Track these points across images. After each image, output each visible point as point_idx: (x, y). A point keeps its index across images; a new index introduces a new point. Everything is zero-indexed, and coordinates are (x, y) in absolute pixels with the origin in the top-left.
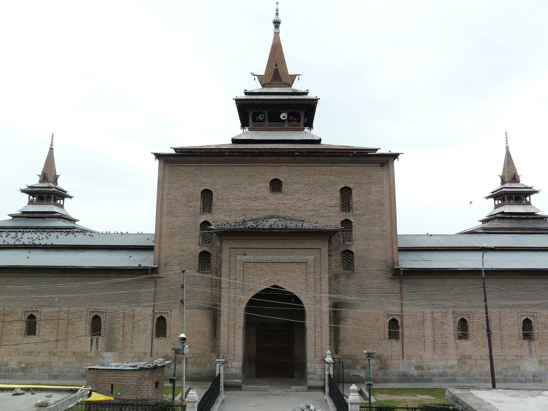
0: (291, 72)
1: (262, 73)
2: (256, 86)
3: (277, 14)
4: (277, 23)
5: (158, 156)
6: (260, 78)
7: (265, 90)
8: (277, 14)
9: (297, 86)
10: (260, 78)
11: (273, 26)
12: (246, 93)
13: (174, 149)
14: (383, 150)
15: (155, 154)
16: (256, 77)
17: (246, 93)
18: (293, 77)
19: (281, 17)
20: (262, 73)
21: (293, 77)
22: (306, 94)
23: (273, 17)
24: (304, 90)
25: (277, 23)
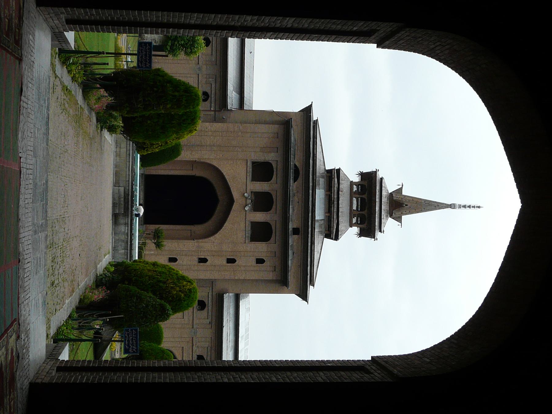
0: (404, 217)
1: (404, 193)
2: (390, 186)
5: (308, 111)
6: (400, 191)
7: (384, 193)
9: (389, 224)
10: (400, 191)
12: (382, 179)
13: (317, 120)
15: (310, 106)
16: (401, 186)
17: (382, 179)
18: (399, 219)
20: (404, 193)
21: (399, 219)
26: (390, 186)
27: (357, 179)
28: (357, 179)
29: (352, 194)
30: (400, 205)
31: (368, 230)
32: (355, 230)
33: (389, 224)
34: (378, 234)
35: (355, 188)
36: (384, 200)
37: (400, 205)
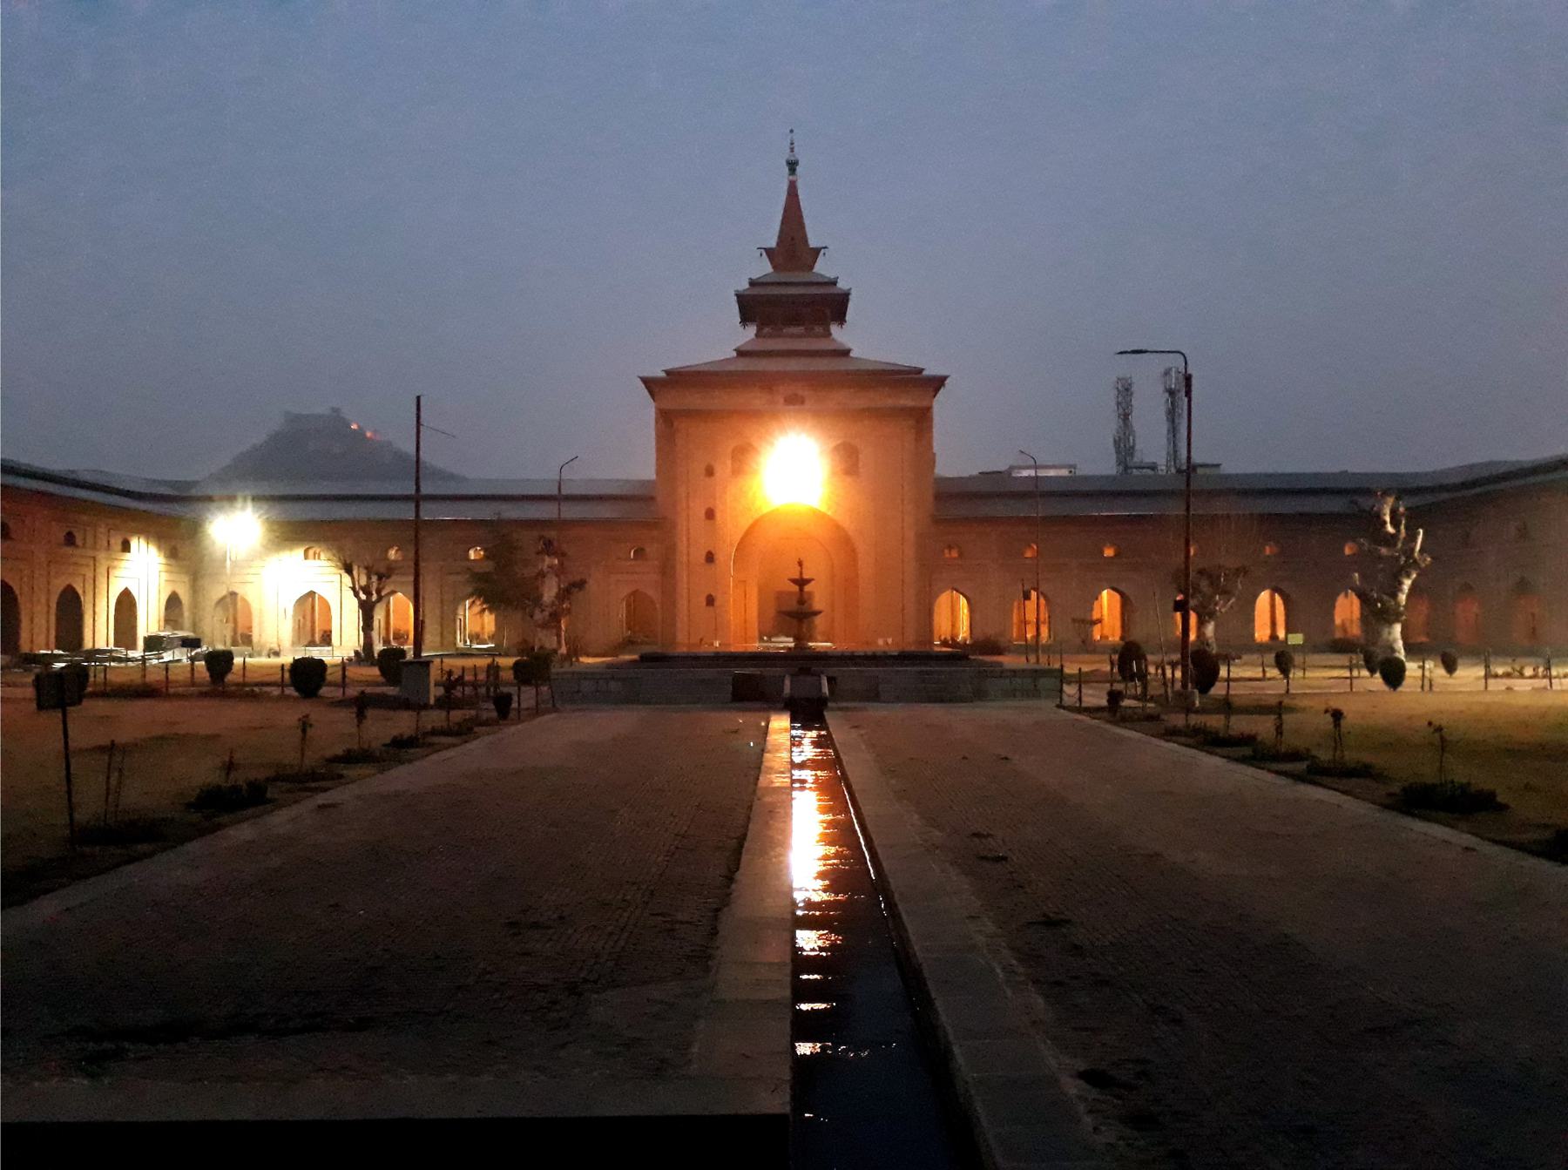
0: (813, 243)
1: (773, 243)
2: (764, 268)
3: (792, 150)
4: (792, 166)
6: (769, 252)
8: (792, 150)
9: (823, 268)
10: (769, 252)
11: (786, 169)
14: (931, 370)
18: (816, 252)
19: (799, 154)
20: (773, 243)
21: (816, 252)
22: (834, 283)
23: (787, 155)
24: (831, 275)
25: (792, 166)
26: (764, 268)
27: (751, 331)
28: (751, 331)
29: (777, 335)
30: (793, 248)
31: (834, 306)
32: (835, 329)
33: (823, 268)
34: (842, 285)
35: (766, 330)
36: (783, 277)
37: (793, 248)
